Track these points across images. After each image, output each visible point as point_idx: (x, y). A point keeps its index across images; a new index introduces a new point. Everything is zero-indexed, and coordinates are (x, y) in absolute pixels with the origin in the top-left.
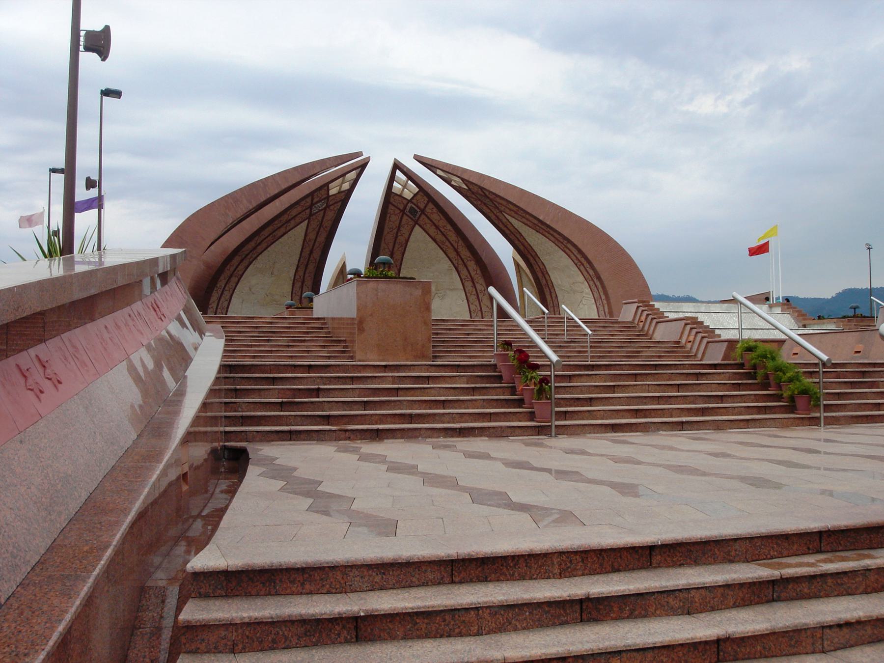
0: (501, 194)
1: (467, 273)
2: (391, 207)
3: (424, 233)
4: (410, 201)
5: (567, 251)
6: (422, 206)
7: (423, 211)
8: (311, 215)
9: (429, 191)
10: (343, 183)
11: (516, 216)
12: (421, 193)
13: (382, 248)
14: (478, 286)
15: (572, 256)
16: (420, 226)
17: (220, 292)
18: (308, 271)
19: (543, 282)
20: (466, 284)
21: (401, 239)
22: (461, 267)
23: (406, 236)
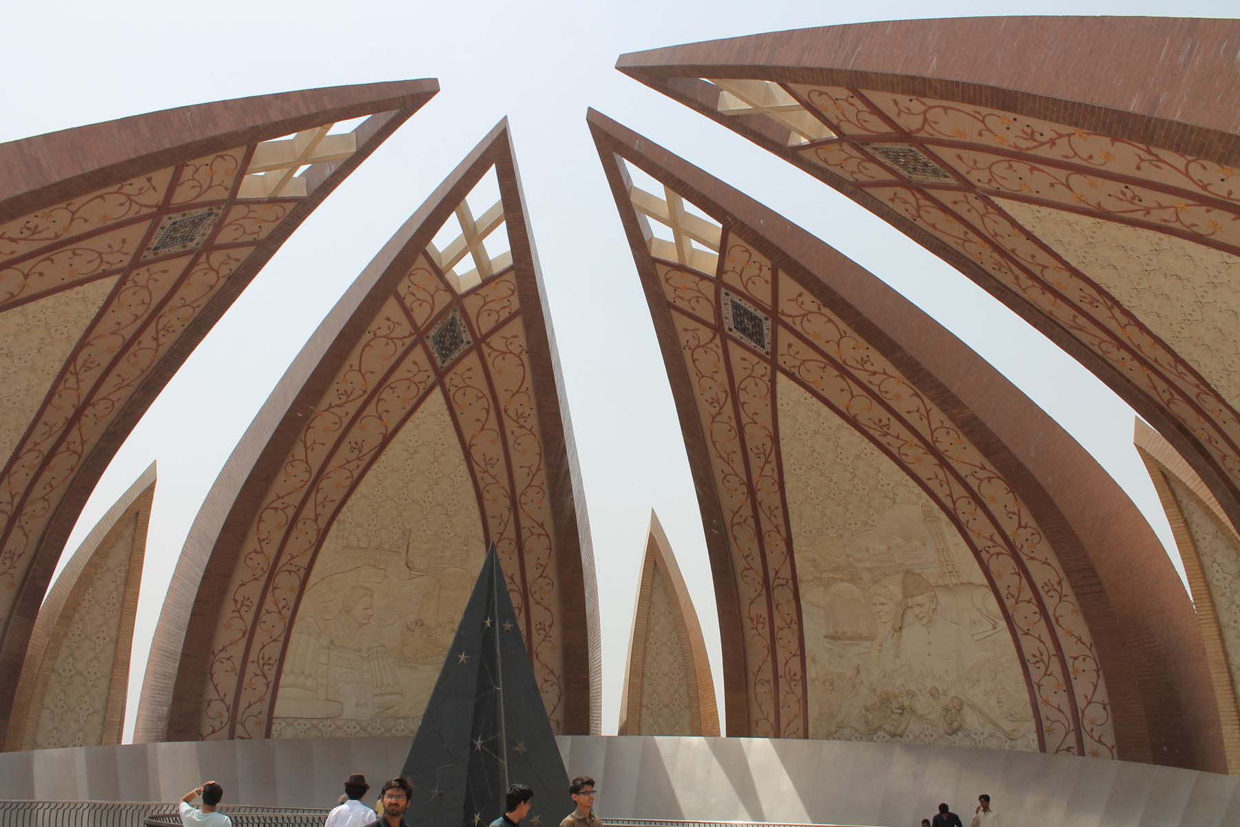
0: (932, 69)
2: (680, 321)
4: (718, 280)
6: (763, 293)
7: (773, 312)
8: (440, 375)
9: (759, 225)
10: (473, 236)
12: (733, 239)
13: (719, 477)
16: (791, 376)
17: (249, 618)
18: (530, 560)
20: (994, 566)
21: (757, 436)
22: (965, 508)
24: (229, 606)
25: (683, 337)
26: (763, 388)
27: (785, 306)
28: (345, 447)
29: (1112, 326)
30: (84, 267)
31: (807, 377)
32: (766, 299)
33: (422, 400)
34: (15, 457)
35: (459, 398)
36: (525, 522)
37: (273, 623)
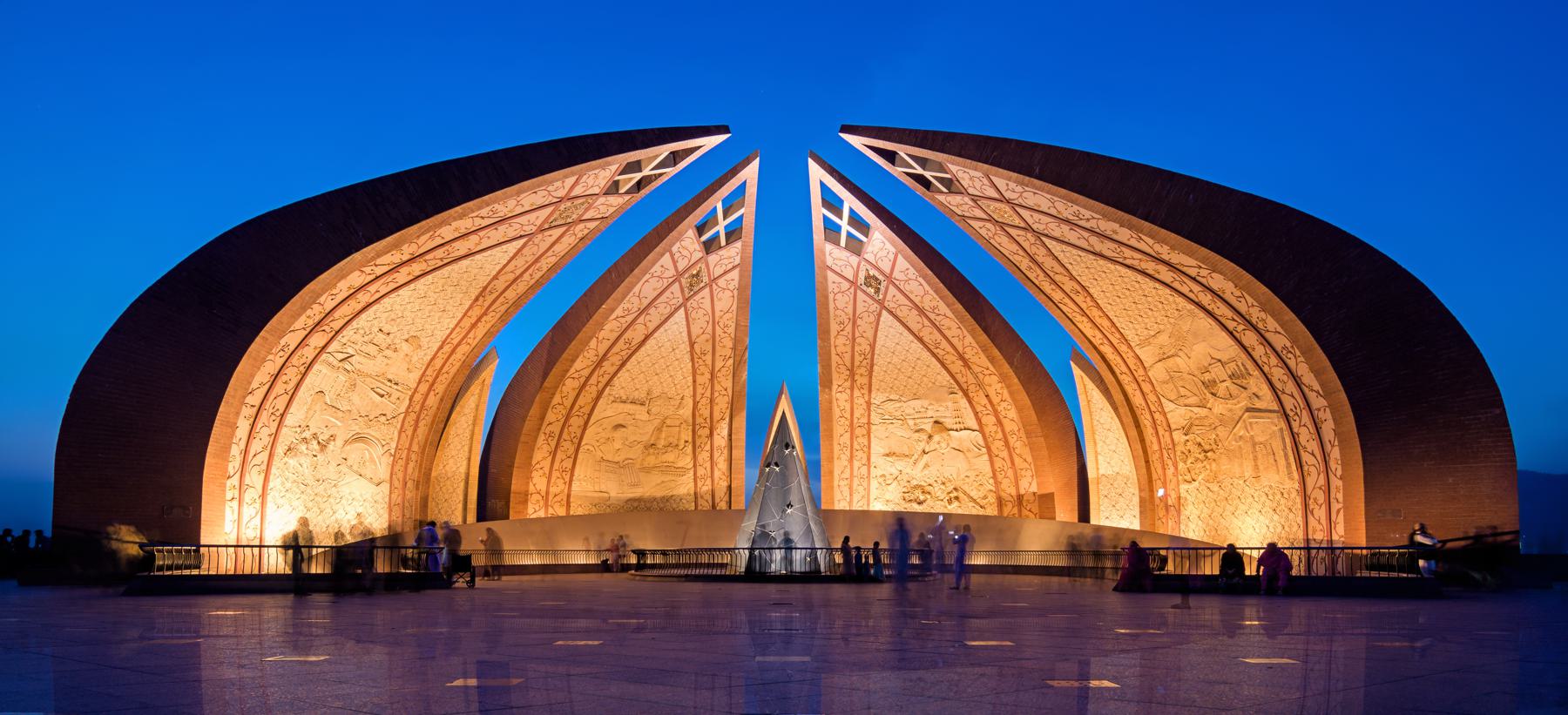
1: (985, 401)
2: (831, 276)
3: (901, 329)
5: (1206, 299)
6: (887, 268)
7: (889, 278)
11: (1072, 236)
13: (834, 365)
14: (1005, 421)
15: (1221, 310)
16: (891, 313)
17: (553, 444)
19: (1137, 400)
20: (984, 420)
21: (863, 346)
23: (870, 334)
24: (542, 437)
25: (831, 287)
26: (872, 319)
27: (896, 274)
28: (622, 341)
29: (1084, 306)
30: (512, 234)
31: (899, 314)
32: (887, 270)
33: (671, 315)
34: (441, 347)
35: (693, 315)
36: (717, 387)
37: (567, 446)
